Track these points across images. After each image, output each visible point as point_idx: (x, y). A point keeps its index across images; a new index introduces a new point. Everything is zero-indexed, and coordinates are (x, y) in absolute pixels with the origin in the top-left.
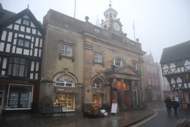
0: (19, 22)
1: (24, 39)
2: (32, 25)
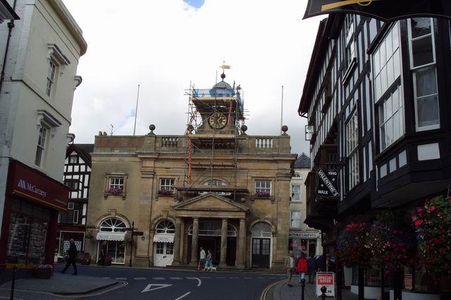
2: (81, 161)
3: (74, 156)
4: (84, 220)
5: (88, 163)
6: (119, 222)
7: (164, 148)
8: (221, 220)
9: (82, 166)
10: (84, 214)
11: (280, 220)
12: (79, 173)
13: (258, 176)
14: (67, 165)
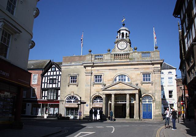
0: (50, 70)
1: (53, 79)
2: (57, 69)
3: (54, 67)
4: (59, 97)
5: (60, 70)
6: (75, 98)
7: (96, 60)
8: (126, 94)
9: (57, 72)
10: (59, 95)
11: (156, 93)
12: (56, 75)
13: (144, 71)
14: (50, 72)
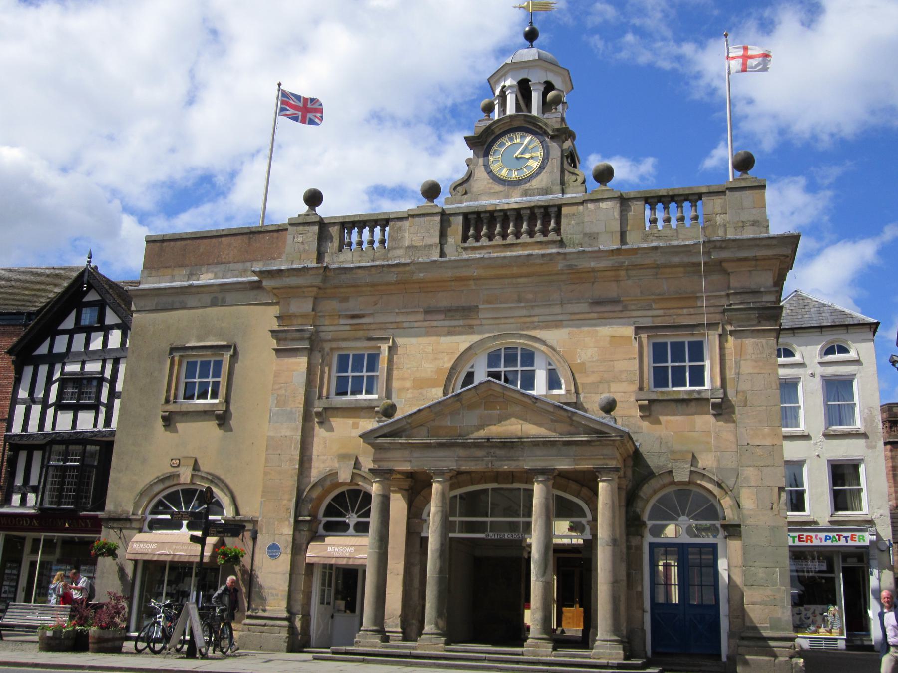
0: (69, 323)
14: (71, 333)
